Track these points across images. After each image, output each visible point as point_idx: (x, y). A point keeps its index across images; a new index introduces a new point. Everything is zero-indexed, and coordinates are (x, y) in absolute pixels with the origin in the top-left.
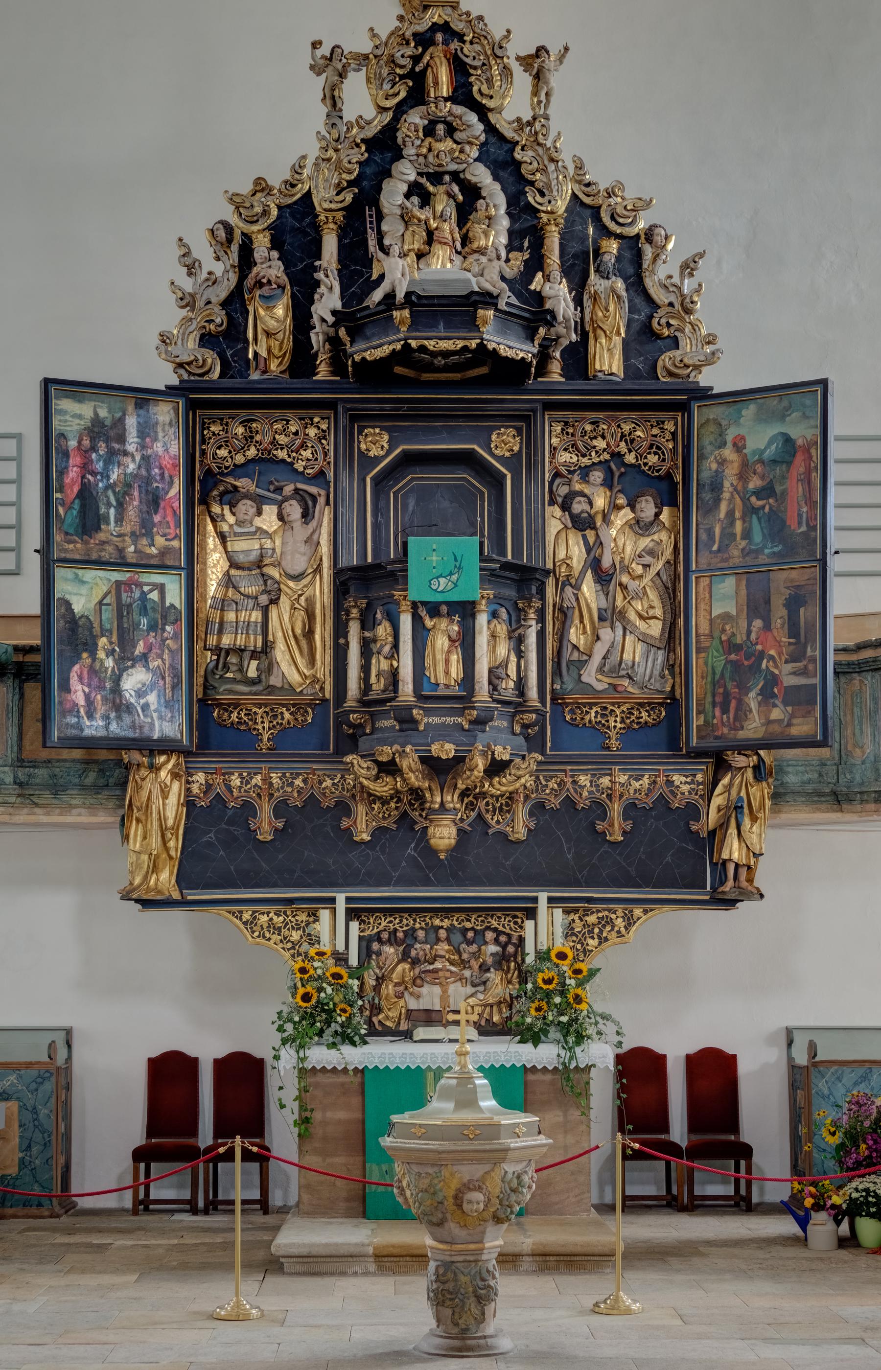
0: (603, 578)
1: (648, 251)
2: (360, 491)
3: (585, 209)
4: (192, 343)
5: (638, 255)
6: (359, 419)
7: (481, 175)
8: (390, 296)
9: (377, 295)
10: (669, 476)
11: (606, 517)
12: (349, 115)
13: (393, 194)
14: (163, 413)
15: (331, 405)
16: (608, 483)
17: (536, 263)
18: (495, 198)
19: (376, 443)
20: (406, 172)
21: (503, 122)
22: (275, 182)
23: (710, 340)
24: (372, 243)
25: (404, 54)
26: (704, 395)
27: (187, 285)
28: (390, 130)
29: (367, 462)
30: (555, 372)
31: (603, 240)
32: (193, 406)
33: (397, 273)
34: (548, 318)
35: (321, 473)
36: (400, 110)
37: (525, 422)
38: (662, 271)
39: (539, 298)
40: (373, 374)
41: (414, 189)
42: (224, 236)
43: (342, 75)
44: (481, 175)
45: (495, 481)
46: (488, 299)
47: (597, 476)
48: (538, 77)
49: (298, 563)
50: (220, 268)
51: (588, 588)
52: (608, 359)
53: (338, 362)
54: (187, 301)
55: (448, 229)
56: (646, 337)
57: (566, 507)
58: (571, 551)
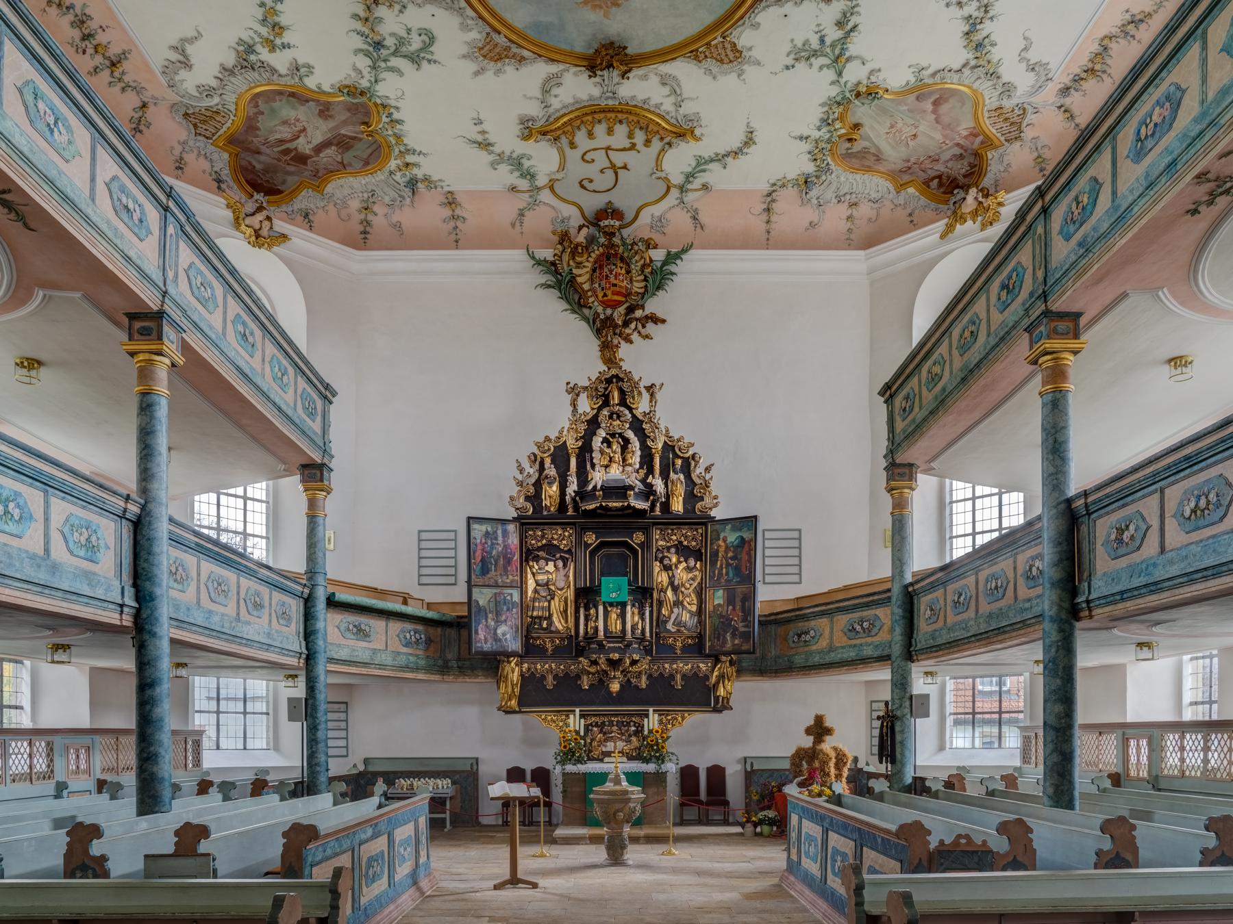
0: (675, 589)
1: (693, 463)
2: (584, 556)
3: (669, 448)
4: (522, 500)
5: (689, 464)
6: (584, 529)
7: (630, 434)
8: (595, 487)
9: (590, 487)
10: (699, 550)
11: (676, 567)
12: (580, 411)
13: (597, 442)
14: (511, 528)
15: (574, 524)
16: (677, 553)
17: (650, 471)
18: (635, 444)
19: (591, 538)
20: (602, 433)
21: (638, 413)
22: (553, 437)
23: (716, 497)
24: (588, 467)
25: (601, 387)
26: (712, 519)
27: (520, 477)
28: (596, 416)
29: (587, 545)
30: (658, 511)
31: (675, 459)
32: (522, 524)
33: (598, 477)
34: (653, 493)
35: (570, 550)
36: (600, 409)
37: (646, 530)
38: (698, 471)
39: (651, 486)
40: (587, 514)
41: (605, 440)
42: (533, 458)
43: (578, 395)
44: (630, 434)
45: (635, 552)
46: (631, 488)
47: (673, 550)
48: (652, 395)
49: (561, 584)
50: (532, 471)
51: (670, 593)
52: (678, 506)
53: (576, 508)
54: (520, 484)
55: (618, 457)
56: (692, 497)
57: (661, 562)
58: (663, 578)
